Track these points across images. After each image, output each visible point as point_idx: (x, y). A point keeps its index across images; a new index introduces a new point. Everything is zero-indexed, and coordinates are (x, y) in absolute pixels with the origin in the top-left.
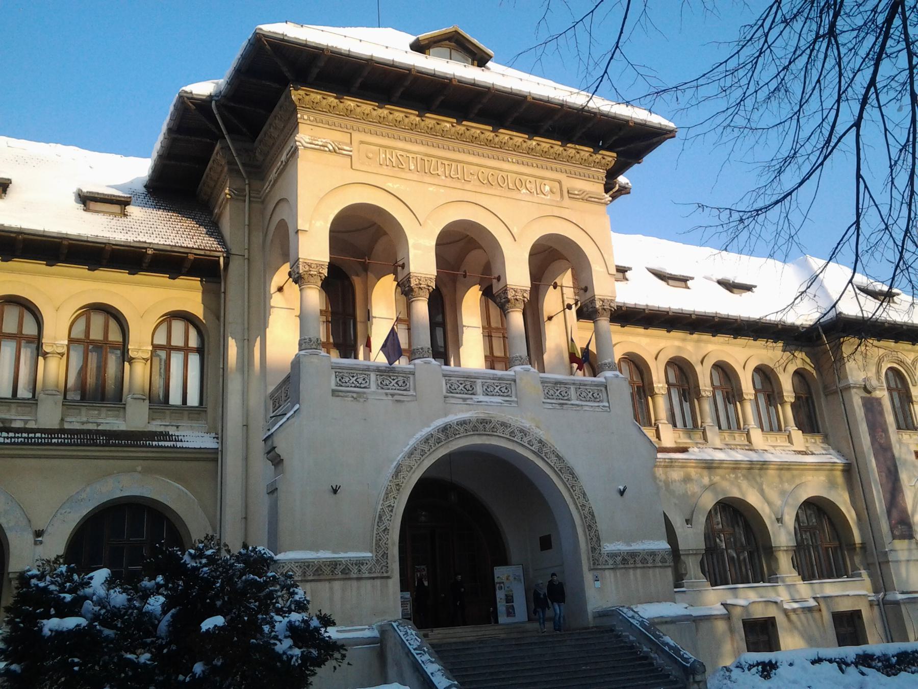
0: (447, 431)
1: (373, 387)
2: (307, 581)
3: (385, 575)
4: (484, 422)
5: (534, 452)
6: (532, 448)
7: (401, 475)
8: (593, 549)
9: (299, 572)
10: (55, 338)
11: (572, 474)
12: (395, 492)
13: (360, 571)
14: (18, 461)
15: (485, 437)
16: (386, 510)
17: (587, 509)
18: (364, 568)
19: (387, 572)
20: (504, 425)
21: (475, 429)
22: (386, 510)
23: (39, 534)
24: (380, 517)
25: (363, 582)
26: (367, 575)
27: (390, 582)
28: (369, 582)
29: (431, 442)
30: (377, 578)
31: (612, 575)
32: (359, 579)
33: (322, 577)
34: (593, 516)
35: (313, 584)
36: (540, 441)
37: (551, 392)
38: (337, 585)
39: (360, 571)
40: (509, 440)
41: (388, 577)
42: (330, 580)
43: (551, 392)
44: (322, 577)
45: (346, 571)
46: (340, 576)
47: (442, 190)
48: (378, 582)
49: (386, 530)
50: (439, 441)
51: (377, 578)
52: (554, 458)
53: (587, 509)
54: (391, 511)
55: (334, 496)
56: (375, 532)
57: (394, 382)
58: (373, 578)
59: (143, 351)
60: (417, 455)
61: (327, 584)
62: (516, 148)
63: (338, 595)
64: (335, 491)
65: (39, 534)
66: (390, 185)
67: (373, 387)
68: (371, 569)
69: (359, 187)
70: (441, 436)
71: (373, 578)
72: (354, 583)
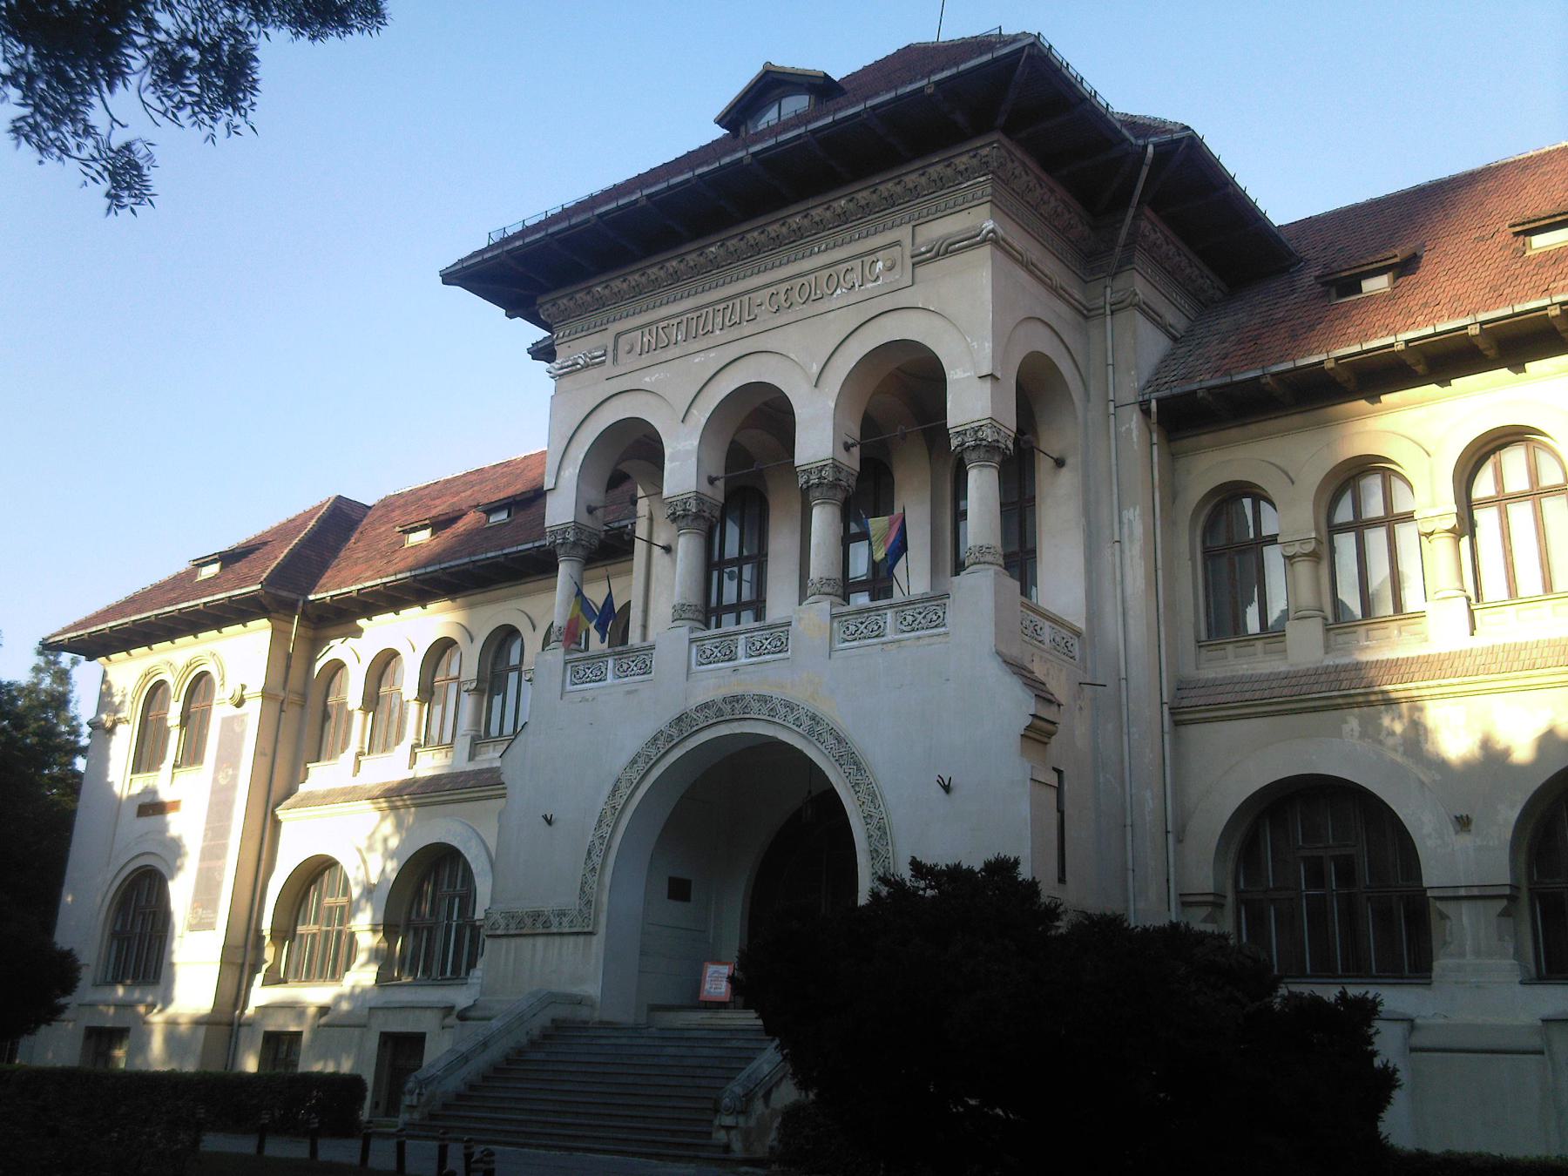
4: (736, 699)
9: (502, 923)
16: (597, 843)
18: (565, 920)
22: (597, 843)
25: (566, 939)
26: (567, 930)
27: (595, 939)
28: (572, 939)
36: (813, 718)
38: (540, 941)
41: (590, 933)
47: (712, 354)
48: (581, 939)
58: (578, 934)
61: (530, 941)
62: (820, 226)
66: (647, 380)
69: (606, 405)
71: (578, 934)
72: (557, 939)
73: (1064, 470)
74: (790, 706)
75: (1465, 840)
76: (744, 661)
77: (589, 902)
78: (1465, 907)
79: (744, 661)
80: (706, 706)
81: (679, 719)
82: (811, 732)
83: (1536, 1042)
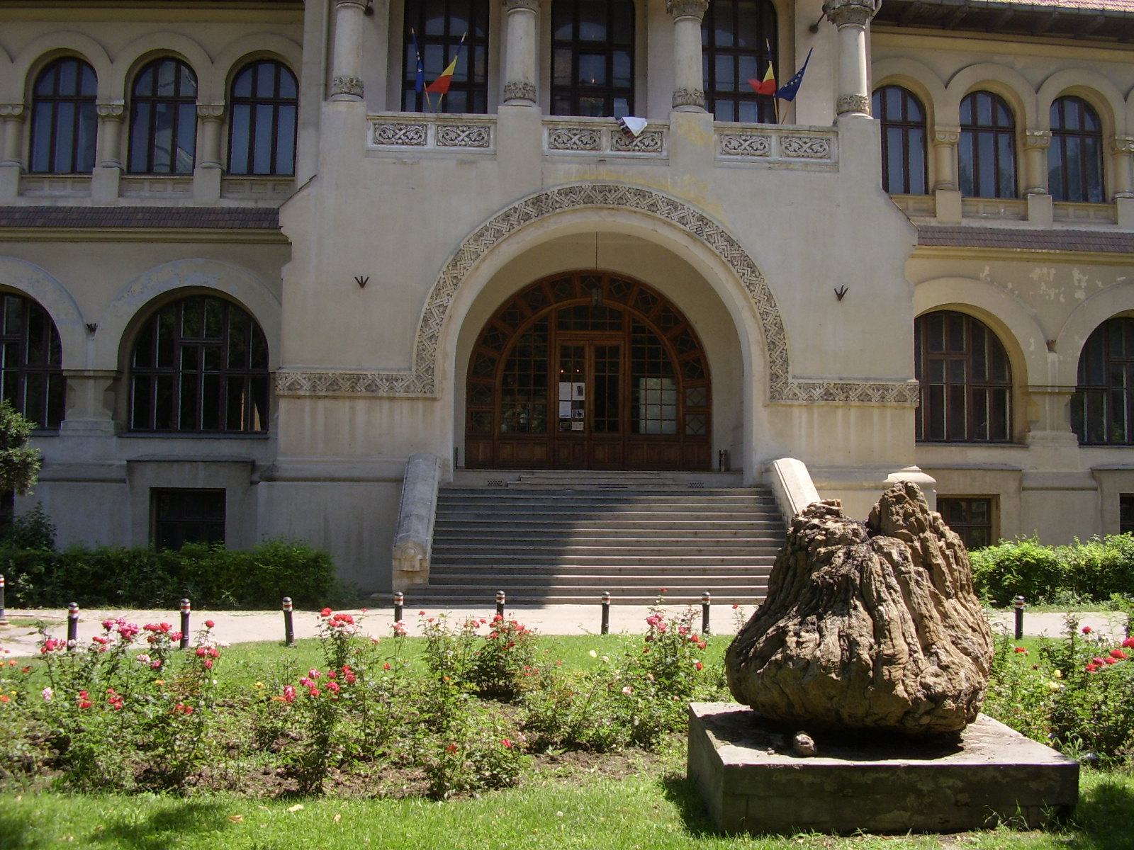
0: (541, 204)
1: (431, 143)
2: (319, 398)
3: (429, 395)
4: (606, 190)
5: (688, 235)
6: (687, 228)
7: (461, 264)
8: (774, 377)
9: (307, 385)
10: (110, 98)
11: (752, 267)
12: (450, 288)
13: (392, 388)
14: (68, 246)
15: (606, 212)
17: (771, 318)
19: (432, 392)
20: (641, 194)
21: (589, 200)
23: (91, 329)
24: (425, 320)
25: (397, 404)
26: (402, 394)
27: (438, 405)
28: (406, 404)
29: (513, 219)
30: (418, 399)
31: (804, 416)
32: (392, 399)
33: (337, 393)
34: (781, 328)
35: (328, 403)
36: (701, 218)
37: (734, 143)
38: (361, 406)
39: (392, 388)
40: (649, 216)
41: (434, 399)
42: (350, 398)
43: (734, 143)
44: (337, 393)
45: (372, 387)
46: (364, 393)
48: (420, 404)
49: (433, 337)
50: (527, 217)
51: (418, 399)
52: (722, 243)
53: (771, 318)
54: (443, 313)
55: (362, 290)
56: (417, 339)
57: (463, 135)
59: (214, 108)
60: (489, 236)
61: (347, 403)
63: (361, 417)
64: (362, 284)
65: (91, 329)
67: (431, 143)
68: (408, 386)
70: (531, 210)
72: (386, 405)
73: (818, 35)
74: (673, 205)
75: (1052, 357)
76: (608, 152)
77: (430, 370)
78: (1047, 398)
79: (608, 152)
80: (571, 191)
81: (537, 201)
82: (699, 232)
83: (1093, 483)
